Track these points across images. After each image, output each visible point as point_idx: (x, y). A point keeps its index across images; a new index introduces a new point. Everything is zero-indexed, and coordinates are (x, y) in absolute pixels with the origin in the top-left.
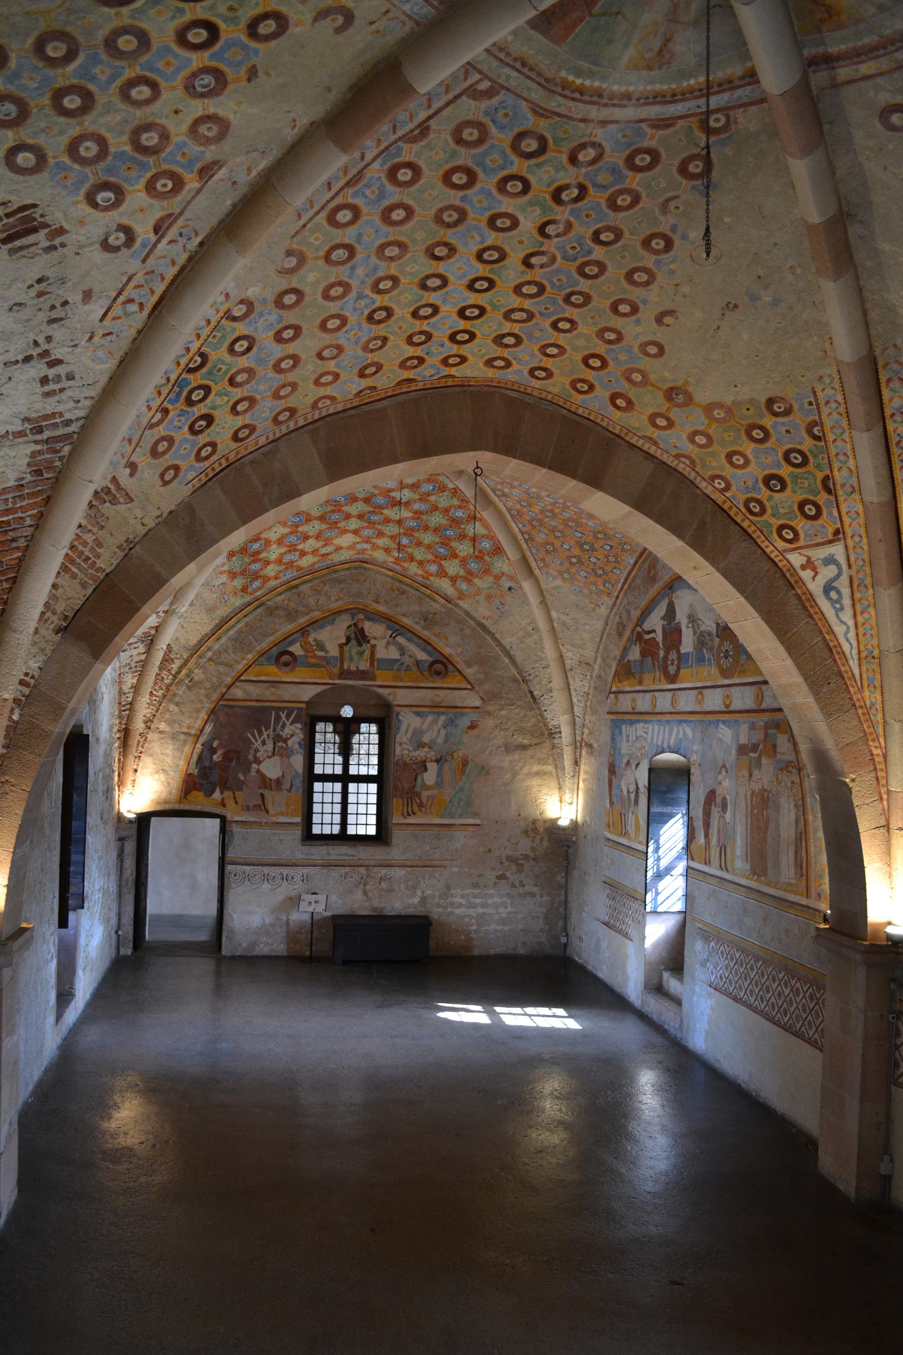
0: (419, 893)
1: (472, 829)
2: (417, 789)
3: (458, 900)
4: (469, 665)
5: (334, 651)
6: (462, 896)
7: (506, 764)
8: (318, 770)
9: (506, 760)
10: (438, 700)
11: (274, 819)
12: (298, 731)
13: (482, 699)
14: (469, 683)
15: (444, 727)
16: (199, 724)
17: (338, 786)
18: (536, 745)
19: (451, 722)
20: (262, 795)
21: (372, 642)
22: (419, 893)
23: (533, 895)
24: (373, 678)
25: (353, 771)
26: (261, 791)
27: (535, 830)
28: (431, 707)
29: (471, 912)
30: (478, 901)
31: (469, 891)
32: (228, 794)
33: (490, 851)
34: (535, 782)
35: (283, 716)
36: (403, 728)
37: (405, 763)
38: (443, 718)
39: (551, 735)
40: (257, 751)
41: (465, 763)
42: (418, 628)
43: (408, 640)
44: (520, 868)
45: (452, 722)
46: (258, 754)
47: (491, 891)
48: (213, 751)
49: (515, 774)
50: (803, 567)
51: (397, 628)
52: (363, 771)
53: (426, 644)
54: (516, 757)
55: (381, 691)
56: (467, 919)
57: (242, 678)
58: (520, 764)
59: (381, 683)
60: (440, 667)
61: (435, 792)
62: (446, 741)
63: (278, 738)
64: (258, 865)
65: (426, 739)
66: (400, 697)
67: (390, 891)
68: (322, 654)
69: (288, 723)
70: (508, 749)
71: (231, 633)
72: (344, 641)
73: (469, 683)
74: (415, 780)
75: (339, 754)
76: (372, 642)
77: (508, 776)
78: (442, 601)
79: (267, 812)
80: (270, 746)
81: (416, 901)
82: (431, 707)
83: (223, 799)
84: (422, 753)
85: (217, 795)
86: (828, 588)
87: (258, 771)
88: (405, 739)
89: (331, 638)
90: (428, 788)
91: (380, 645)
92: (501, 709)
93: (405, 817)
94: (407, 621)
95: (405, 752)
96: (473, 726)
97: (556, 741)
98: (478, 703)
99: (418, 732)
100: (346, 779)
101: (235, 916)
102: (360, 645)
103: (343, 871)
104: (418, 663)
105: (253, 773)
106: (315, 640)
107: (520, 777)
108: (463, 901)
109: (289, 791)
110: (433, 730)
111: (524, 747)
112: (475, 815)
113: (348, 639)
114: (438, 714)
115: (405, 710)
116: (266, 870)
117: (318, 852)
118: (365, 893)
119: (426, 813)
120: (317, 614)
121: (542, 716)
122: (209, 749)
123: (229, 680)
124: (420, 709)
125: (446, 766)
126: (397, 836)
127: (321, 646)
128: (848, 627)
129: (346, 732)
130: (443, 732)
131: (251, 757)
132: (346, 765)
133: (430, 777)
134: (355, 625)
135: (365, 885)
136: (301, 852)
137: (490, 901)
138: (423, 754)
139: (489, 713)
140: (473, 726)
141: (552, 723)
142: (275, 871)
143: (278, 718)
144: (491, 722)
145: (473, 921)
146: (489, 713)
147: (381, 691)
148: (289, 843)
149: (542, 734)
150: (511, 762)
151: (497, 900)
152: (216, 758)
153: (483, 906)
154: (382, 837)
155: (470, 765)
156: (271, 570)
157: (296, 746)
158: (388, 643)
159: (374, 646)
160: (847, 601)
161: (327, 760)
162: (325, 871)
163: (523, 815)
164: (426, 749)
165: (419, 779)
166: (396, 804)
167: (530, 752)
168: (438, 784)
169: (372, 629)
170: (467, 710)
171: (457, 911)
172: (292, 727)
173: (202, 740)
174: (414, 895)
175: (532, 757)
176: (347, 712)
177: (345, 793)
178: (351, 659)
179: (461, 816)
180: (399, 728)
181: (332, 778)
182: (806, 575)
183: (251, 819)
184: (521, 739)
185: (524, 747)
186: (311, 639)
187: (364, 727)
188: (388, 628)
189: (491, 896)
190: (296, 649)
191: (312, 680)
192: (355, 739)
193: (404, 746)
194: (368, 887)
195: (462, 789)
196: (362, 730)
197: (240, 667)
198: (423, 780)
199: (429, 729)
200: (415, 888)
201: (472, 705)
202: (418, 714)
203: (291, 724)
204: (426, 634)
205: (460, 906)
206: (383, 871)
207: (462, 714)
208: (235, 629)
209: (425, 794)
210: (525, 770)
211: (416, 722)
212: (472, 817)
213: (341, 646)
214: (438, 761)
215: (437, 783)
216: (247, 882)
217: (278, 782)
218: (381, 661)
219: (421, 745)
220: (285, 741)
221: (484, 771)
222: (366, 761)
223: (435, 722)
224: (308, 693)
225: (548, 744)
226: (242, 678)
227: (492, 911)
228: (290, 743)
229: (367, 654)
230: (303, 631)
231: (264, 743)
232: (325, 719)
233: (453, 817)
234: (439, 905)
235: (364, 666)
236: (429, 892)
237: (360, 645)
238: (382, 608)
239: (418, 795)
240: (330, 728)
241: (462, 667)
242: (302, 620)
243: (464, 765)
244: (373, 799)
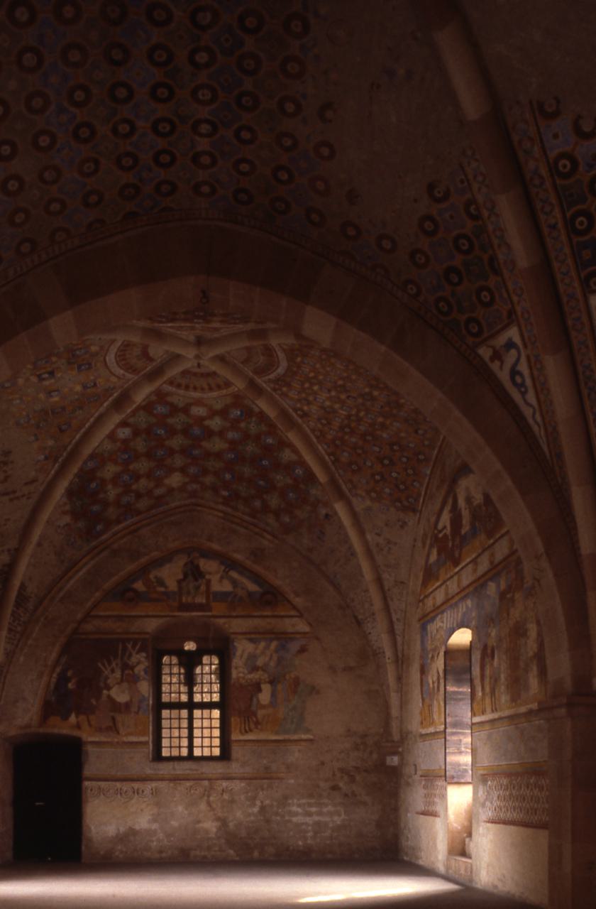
0: (258, 803)
2: (254, 708)
3: (294, 809)
4: (297, 595)
5: (172, 585)
6: (299, 806)
8: (165, 698)
11: (125, 739)
12: (143, 659)
14: (298, 611)
15: (276, 651)
16: (54, 655)
17: (184, 713)
20: (113, 719)
21: (207, 577)
22: (258, 803)
23: (365, 804)
24: (210, 610)
25: (197, 698)
26: (112, 714)
29: (308, 820)
30: (314, 809)
31: (304, 801)
32: (82, 718)
33: (323, 763)
35: (129, 646)
36: (239, 653)
38: (274, 644)
40: (107, 678)
42: (248, 563)
43: (241, 573)
44: (352, 780)
46: (109, 681)
47: (326, 801)
48: (68, 680)
50: (492, 359)
51: (229, 564)
52: (207, 699)
53: (256, 578)
56: (304, 827)
57: (92, 613)
60: (270, 598)
63: (125, 667)
64: (112, 780)
66: (236, 625)
67: (232, 801)
68: (162, 589)
69: (134, 653)
71: (81, 573)
72: (181, 576)
73: (298, 611)
74: (251, 700)
75: (185, 684)
76: (207, 577)
78: (269, 537)
79: (118, 733)
80: (118, 674)
81: (256, 810)
83: (78, 722)
84: (255, 676)
85: (73, 719)
86: (514, 373)
87: (109, 696)
89: (170, 575)
90: (264, 707)
91: (215, 579)
94: (238, 556)
95: (241, 675)
96: (303, 650)
98: (307, 629)
99: (252, 657)
100: (191, 706)
101: (93, 828)
102: (196, 580)
103: (188, 784)
104: (250, 594)
105: (104, 698)
106: (156, 577)
108: (300, 810)
109: (137, 713)
110: (265, 653)
112: (308, 731)
113: (186, 576)
114: (272, 640)
115: (240, 637)
116: (118, 785)
117: (165, 769)
118: (209, 804)
119: (261, 730)
120: (155, 554)
122: (63, 679)
123: (79, 616)
124: (253, 636)
125: (279, 687)
126: (236, 751)
127: (161, 582)
128: (534, 408)
129: (190, 663)
130: (275, 657)
131: (102, 685)
132: (191, 694)
133: (265, 696)
134: (192, 562)
135: (209, 796)
136: (149, 770)
137: (325, 810)
138: (257, 676)
140: (303, 650)
142: (126, 786)
143: (125, 649)
145: (310, 828)
148: (139, 762)
151: (330, 808)
152: (70, 686)
153: (320, 814)
154: (226, 754)
156: (112, 512)
157: (142, 673)
158: (222, 578)
159: (209, 582)
160: (528, 382)
161: (173, 689)
162: (172, 785)
164: (260, 672)
165: (255, 700)
166: (234, 721)
168: (273, 703)
169: (208, 566)
170: (298, 636)
171: (295, 819)
172: (138, 656)
173: (58, 670)
174: (254, 805)
176: (190, 646)
177: (191, 719)
178: (189, 593)
180: (234, 654)
181: (178, 706)
182: (495, 366)
183: (103, 739)
186: (151, 576)
187: (206, 659)
188: (222, 563)
189: (326, 805)
190: (139, 586)
191: (154, 613)
192: (198, 670)
193: (241, 669)
194: (211, 799)
196: (204, 662)
197: (89, 604)
198: (258, 701)
199: (263, 653)
200: (254, 798)
201: (302, 630)
202: (251, 640)
203: (137, 653)
204: (258, 568)
205: (296, 814)
206: (225, 784)
208: (84, 570)
209: (260, 713)
211: (250, 647)
213: (179, 582)
214: (272, 682)
216: (102, 796)
217: (127, 705)
218: (216, 594)
219: (255, 669)
220: (132, 668)
222: (208, 690)
223: (267, 647)
224: (152, 625)
226: (92, 613)
227: (327, 819)
228: (136, 670)
229: (203, 588)
230: (144, 571)
231: (113, 671)
232: (170, 653)
234: (277, 814)
235: (201, 600)
236: (267, 802)
237: (196, 580)
238: (215, 546)
239: (255, 714)
240: (175, 660)
241: (291, 597)
242: (143, 560)
244: (216, 723)
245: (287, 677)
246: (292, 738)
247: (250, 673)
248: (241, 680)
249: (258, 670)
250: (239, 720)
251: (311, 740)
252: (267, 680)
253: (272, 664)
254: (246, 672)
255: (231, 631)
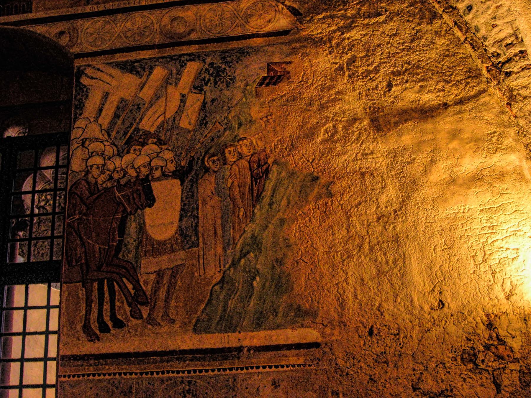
1: (293, 358)
7: (380, 162)
9: (380, 151)
10: (180, 29)
13: (294, 12)
15: (198, 88)
18: (461, 102)
19: (216, 75)
27: (496, 342)
28: (161, 46)
34: (474, 201)
37: (93, 188)
38: (192, 69)
39: (499, 69)
41: (260, 171)
45: (218, 73)
49: (409, 186)
54: (407, 139)
55: (40, 29)
58: (422, 158)
59: (41, 15)
61: (180, 257)
62: (203, 122)
65: (149, 123)
70: (382, 121)
74: (122, 229)
77: (391, 192)
82: (161, 46)
84: (137, 160)
88: (94, 131)
90: (158, 248)
92: (349, 28)
93: (93, 337)
97: (514, 83)
98: (283, 22)
99: (129, 110)
107: (427, 192)
111: (425, 113)
112: (301, 315)
114: (181, 62)
115: (95, 62)
119: (151, 321)
121: (465, 27)
124: (133, 56)
125: (207, 186)
130: (194, 101)
133: (161, 220)
138: (140, 161)
139: (317, 42)
140: (274, 78)
141: (495, 35)
144: (323, 62)
146: (317, 42)
147: (40, 29)
149: (473, 74)
150: (394, 154)
155: (273, 176)
163: (452, 305)
164: (152, 148)
165: (132, 227)
167: (445, 123)
168: (188, 235)
175: (455, 134)
179: (259, 323)
180: (81, 106)
184: (409, 95)
185: (425, 113)
195: (255, 243)
198: (142, 228)
199: (157, 97)
201: (269, 28)
202: (128, 67)
207: (243, 52)
209: (149, 267)
210: (440, 173)
212: (293, 324)
214: (180, 174)
215: (182, 232)
219: (134, 139)
221: (317, 185)
223: (171, 80)
225: (495, 96)
233: (233, 328)
243: (255, 178)
245: (231, 159)
246: (246, 343)
247: (120, 155)
248: (95, 172)
249: (143, 144)
250: (82, 293)
251: (316, 345)
252: (171, 167)
253: (187, 122)
254: (109, 150)
255: (75, 50)
